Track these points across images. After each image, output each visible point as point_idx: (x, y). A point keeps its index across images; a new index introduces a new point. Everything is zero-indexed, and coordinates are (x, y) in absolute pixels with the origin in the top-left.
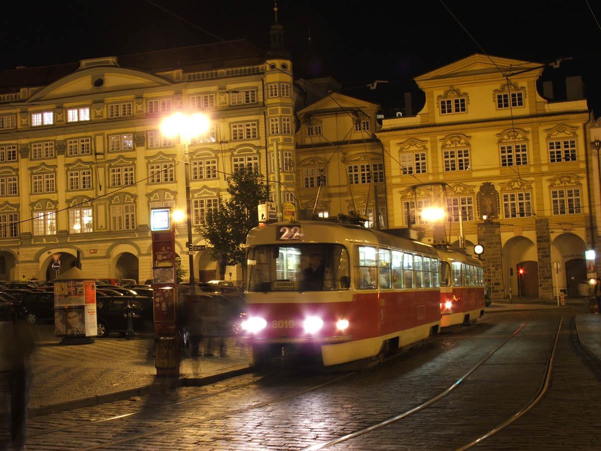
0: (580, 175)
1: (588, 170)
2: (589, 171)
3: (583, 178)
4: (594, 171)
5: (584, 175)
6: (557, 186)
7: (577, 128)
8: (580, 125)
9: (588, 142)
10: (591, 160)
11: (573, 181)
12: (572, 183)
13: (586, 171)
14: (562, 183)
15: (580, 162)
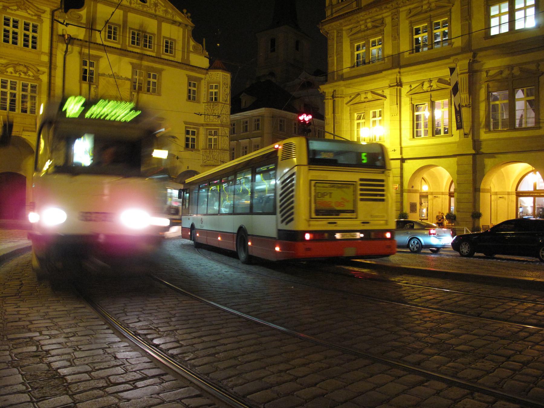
0: (41, 69)
1: (51, 66)
2: (52, 66)
3: (44, 73)
4: (58, 68)
5: (46, 70)
6: (8, 74)
7: (44, 12)
8: (48, 10)
9: (55, 33)
10: (56, 55)
11: (30, 73)
12: (29, 76)
13: (48, 65)
14: (16, 72)
15: (43, 53)
